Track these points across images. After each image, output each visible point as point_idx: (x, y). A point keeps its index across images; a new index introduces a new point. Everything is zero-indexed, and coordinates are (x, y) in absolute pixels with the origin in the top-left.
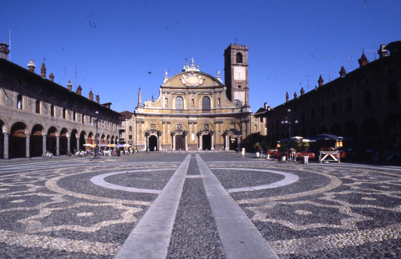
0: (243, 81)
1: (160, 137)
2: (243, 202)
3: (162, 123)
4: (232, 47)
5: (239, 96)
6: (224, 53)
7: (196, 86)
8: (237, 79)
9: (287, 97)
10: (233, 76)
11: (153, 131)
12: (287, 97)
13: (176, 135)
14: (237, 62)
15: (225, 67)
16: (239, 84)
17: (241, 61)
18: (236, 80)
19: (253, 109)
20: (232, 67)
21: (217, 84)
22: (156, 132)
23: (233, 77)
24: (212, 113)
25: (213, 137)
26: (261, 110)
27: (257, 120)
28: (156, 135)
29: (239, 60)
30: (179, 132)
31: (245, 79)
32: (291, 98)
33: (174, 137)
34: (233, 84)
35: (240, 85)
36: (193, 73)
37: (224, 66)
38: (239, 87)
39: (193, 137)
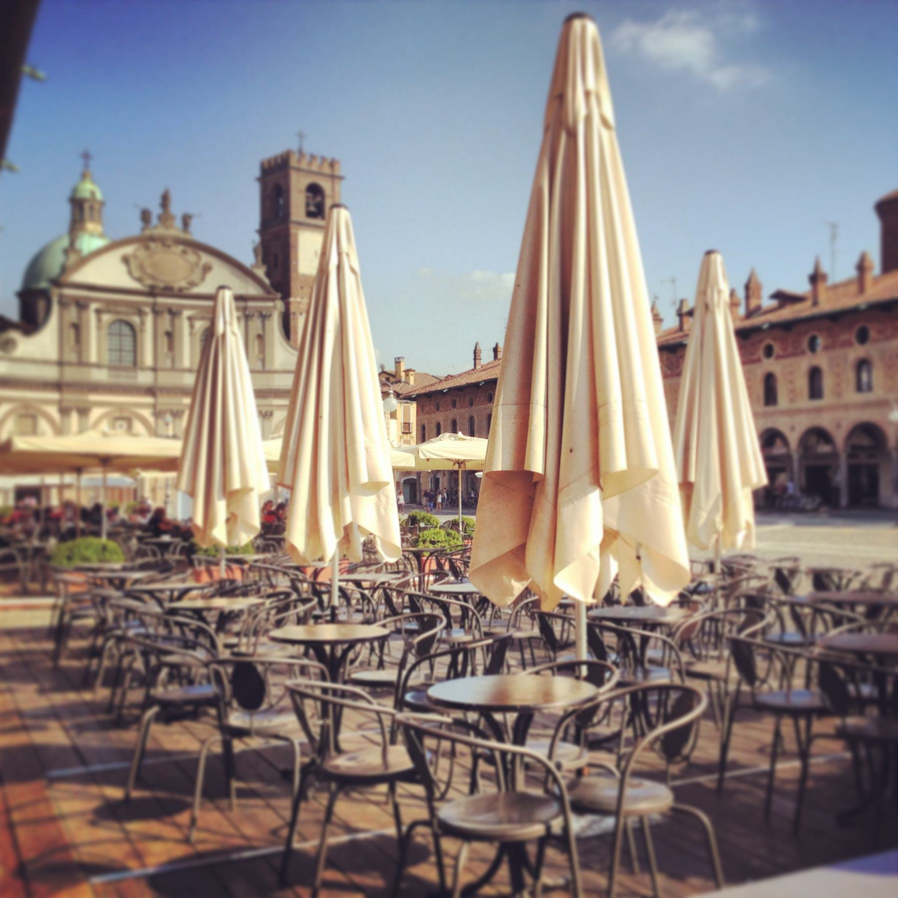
10: (297, 260)
23: (296, 266)
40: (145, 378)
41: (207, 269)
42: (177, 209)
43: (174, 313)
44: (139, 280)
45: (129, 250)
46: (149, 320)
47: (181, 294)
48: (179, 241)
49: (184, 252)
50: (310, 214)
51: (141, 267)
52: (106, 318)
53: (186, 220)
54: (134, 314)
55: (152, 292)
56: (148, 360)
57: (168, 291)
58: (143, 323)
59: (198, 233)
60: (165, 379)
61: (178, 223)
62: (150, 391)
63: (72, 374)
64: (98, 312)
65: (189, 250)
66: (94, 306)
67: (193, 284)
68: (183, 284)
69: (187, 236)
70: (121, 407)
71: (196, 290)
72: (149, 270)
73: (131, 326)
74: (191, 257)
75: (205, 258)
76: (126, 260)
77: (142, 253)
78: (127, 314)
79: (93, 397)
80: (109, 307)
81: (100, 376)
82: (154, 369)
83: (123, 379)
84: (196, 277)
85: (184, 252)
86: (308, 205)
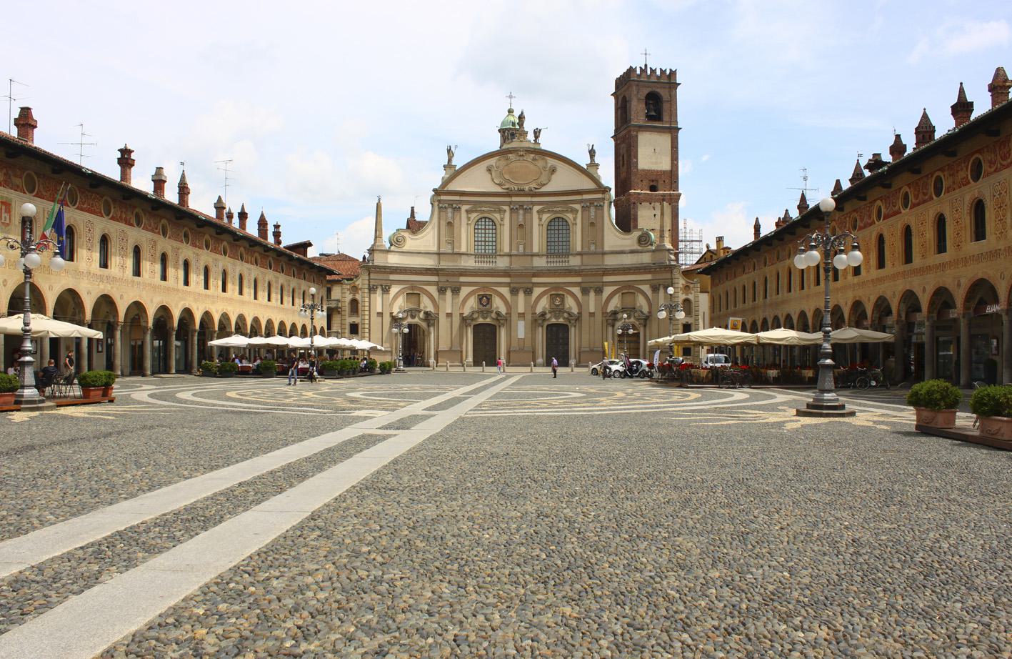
0: (664, 172)
1: (432, 329)
5: (647, 218)
8: (646, 167)
11: (412, 313)
13: (474, 323)
14: (650, 118)
15: (616, 130)
16: (653, 181)
17: (658, 118)
18: (644, 170)
19: (689, 260)
21: (590, 185)
22: (422, 315)
24: (575, 262)
25: (572, 331)
27: (692, 286)
28: (424, 325)
29: (654, 114)
35: (654, 184)
36: (522, 153)
37: (613, 128)
38: (653, 188)
39: (521, 329)
40: (502, 263)
41: (553, 171)
42: (529, 127)
44: (499, 185)
45: (492, 161)
46: (507, 215)
48: (529, 151)
49: (534, 159)
50: (650, 118)
51: (501, 175)
52: (474, 216)
53: (537, 133)
54: (495, 212)
56: (506, 250)
57: (521, 193)
58: (502, 219)
59: (545, 144)
61: (531, 137)
62: (506, 273)
64: (467, 211)
65: (537, 157)
66: (464, 208)
68: (534, 185)
69: (537, 147)
70: (485, 286)
71: (544, 189)
72: (507, 177)
74: (540, 163)
75: (551, 162)
76: (489, 170)
77: (503, 163)
78: (489, 212)
80: (475, 207)
82: (510, 255)
84: (543, 179)
85: (534, 159)
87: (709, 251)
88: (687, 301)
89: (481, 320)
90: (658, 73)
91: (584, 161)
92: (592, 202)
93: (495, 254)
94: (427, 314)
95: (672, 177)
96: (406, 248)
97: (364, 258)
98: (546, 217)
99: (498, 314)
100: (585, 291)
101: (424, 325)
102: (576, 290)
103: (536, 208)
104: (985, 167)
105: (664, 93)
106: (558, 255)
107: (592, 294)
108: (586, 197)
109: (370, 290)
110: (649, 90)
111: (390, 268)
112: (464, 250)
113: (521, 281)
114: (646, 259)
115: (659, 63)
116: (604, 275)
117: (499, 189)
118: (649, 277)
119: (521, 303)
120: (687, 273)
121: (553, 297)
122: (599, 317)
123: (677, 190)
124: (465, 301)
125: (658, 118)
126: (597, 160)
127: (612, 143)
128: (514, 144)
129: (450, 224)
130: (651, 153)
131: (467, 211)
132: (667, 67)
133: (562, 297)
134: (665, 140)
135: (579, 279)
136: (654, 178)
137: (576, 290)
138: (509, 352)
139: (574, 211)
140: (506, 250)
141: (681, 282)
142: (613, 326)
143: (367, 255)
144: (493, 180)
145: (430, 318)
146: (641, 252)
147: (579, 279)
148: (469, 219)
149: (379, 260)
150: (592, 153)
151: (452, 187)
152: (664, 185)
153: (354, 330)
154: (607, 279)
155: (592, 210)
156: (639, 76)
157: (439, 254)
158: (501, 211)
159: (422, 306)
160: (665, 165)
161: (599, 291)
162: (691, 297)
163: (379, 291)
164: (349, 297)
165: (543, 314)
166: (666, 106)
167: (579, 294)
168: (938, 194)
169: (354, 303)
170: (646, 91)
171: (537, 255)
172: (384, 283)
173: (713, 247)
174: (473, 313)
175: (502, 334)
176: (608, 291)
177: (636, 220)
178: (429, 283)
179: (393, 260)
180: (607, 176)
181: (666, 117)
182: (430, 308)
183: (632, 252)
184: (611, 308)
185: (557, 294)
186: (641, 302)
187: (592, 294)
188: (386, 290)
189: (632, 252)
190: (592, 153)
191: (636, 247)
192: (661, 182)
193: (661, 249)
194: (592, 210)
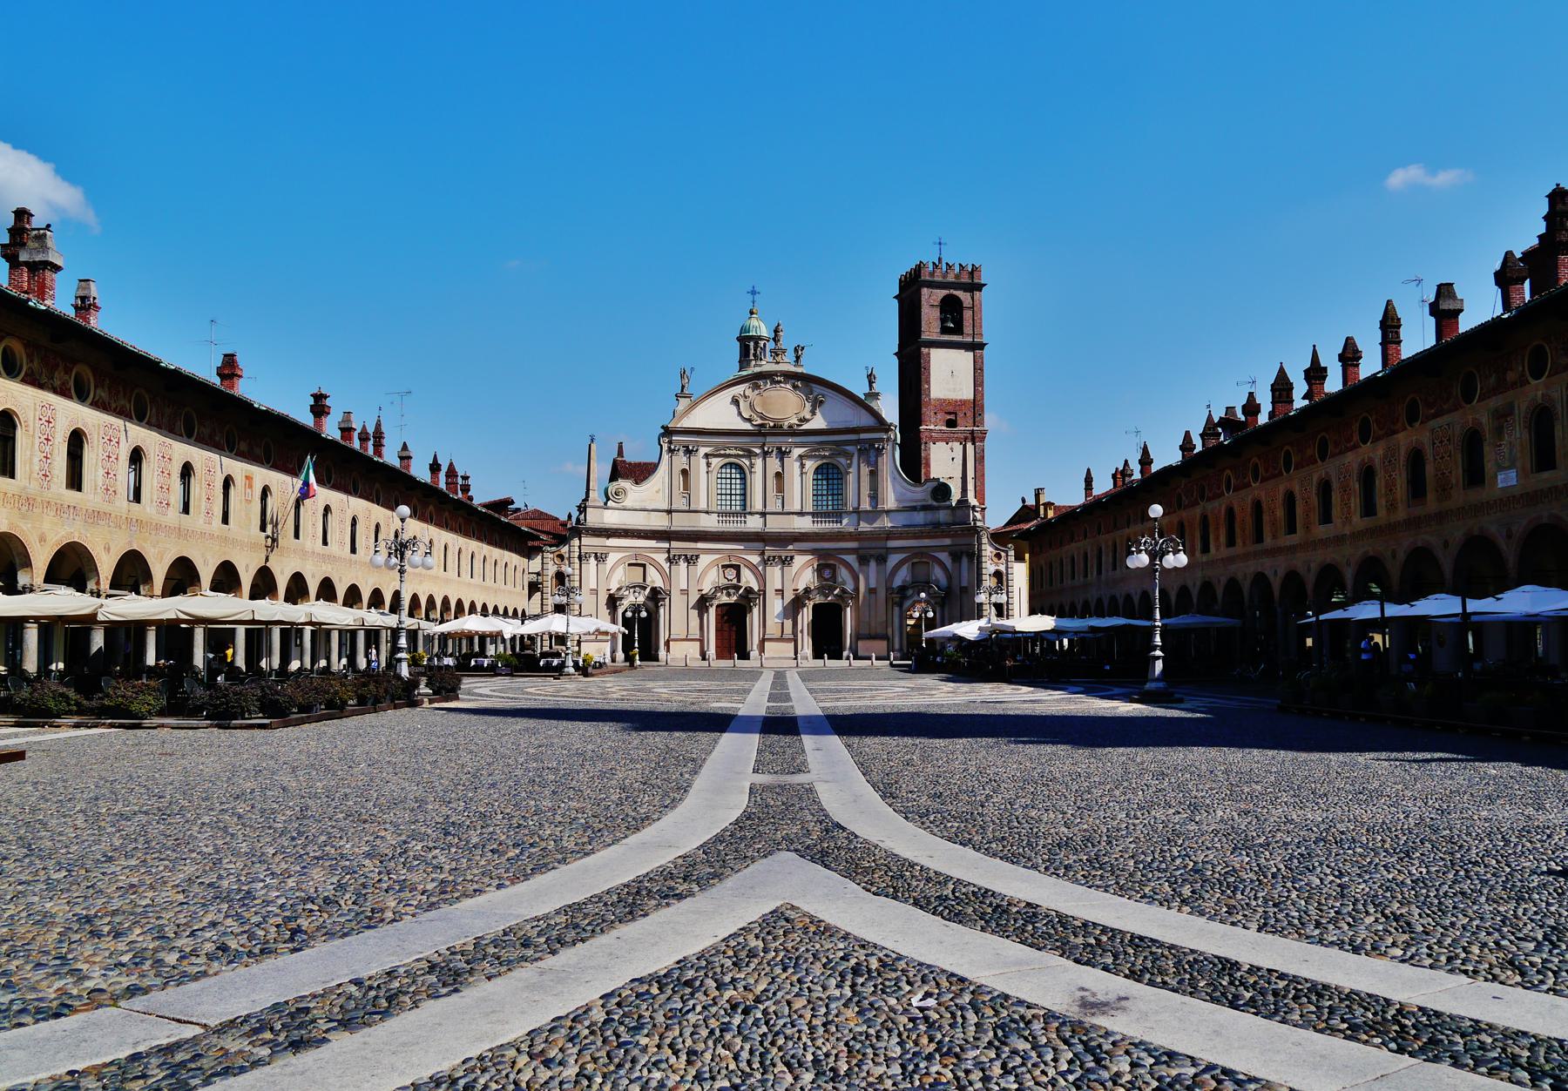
0: (963, 403)
2: (814, 685)
3: (669, 560)
4: (925, 277)
5: (943, 461)
6: (897, 292)
7: (790, 427)
9: (1089, 481)
10: (928, 382)
12: (1089, 481)
13: (716, 602)
14: (945, 330)
17: (958, 330)
19: (996, 514)
20: (924, 350)
21: (866, 420)
26: (1025, 513)
30: (729, 595)
31: (967, 394)
32: (1103, 486)
33: (712, 611)
34: (927, 412)
38: (951, 424)
40: (754, 524)
42: (787, 342)
43: (782, 455)
44: (749, 420)
45: (738, 390)
46: (759, 462)
47: (792, 432)
48: (789, 376)
50: (945, 330)
51: (751, 406)
52: (714, 461)
55: (760, 432)
56: (758, 506)
57: (778, 430)
58: (752, 465)
60: (776, 525)
61: (790, 356)
63: (681, 523)
66: (703, 451)
67: (804, 420)
68: (794, 421)
69: (799, 370)
71: (806, 426)
73: (740, 468)
75: (817, 389)
76: (735, 402)
79: (700, 545)
81: (710, 523)
82: (763, 514)
83: (732, 526)
86: (943, 321)
87: (1024, 507)
88: (998, 574)
89: (724, 599)
90: (957, 269)
91: (860, 390)
92: (871, 442)
93: (745, 512)
94: (654, 590)
95: (976, 407)
96: (628, 503)
97: (570, 516)
98: (811, 465)
99: (749, 590)
100: (863, 560)
101: (650, 604)
102: (851, 559)
103: (797, 452)
104: (1331, 447)
105: (964, 296)
106: (826, 515)
107: (873, 564)
108: (863, 436)
109: (580, 558)
110: (945, 292)
111: (606, 530)
112: (703, 506)
113: (775, 545)
114: (943, 516)
115: (958, 255)
116: (888, 538)
117: (748, 426)
118: (947, 541)
119: (774, 575)
120: (999, 538)
121: (819, 570)
122: (882, 594)
123: (982, 424)
124: (704, 572)
125: (958, 330)
126: (877, 387)
127: (896, 361)
128: (767, 365)
129: (685, 472)
130: (948, 373)
131: (707, 456)
132: (969, 263)
133: (833, 568)
134: (966, 358)
135: (853, 545)
136: (950, 409)
137: (851, 559)
138: (763, 641)
139: (849, 456)
140: (758, 506)
141: (988, 550)
142: (901, 605)
143: (575, 514)
144: (740, 414)
145: (656, 596)
146: (938, 508)
147: (853, 545)
148: (708, 465)
149: (594, 518)
150: (871, 379)
151: (686, 423)
152: (966, 420)
153: (560, 609)
154: (892, 544)
155: (872, 453)
156: (932, 275)
157: (669, 512)
158: (750, 454)
159: (648, 580)
160: (967, 394)
161: (882, 560)
162: (1002, 568)
163: (592, 559)
164: (552, 569)
165: (807, 590)
166: (967, 314)
167: (856, 565)
168: (1288, 471)
169: (560, 577)
170: (942, 293)
171: (801, 514)
172: (599, 551)
173: (1031, 501)
174: (718, 589)
175: (755, 616)
176: (893, 560)
177: (928, 465)
178: (657, 550)
179: (611, 518)
180: (889, 409)
181: (967, 329)
182: (659, 583)
183: (925, 508)
184: (898, 582)
185: (826, 566)
186: (938, 573)
187: (873, 564)
188: (600, 558)
189: (925, 508)
190: (871, 379)
191: (931, 502)
192: (960, 415)
193: (963, 502)
194: (872, 453)
